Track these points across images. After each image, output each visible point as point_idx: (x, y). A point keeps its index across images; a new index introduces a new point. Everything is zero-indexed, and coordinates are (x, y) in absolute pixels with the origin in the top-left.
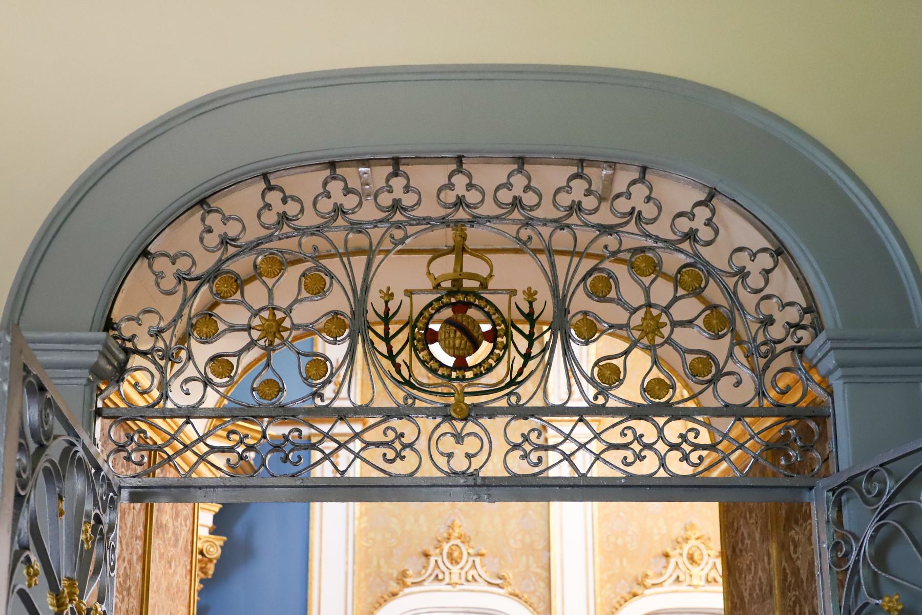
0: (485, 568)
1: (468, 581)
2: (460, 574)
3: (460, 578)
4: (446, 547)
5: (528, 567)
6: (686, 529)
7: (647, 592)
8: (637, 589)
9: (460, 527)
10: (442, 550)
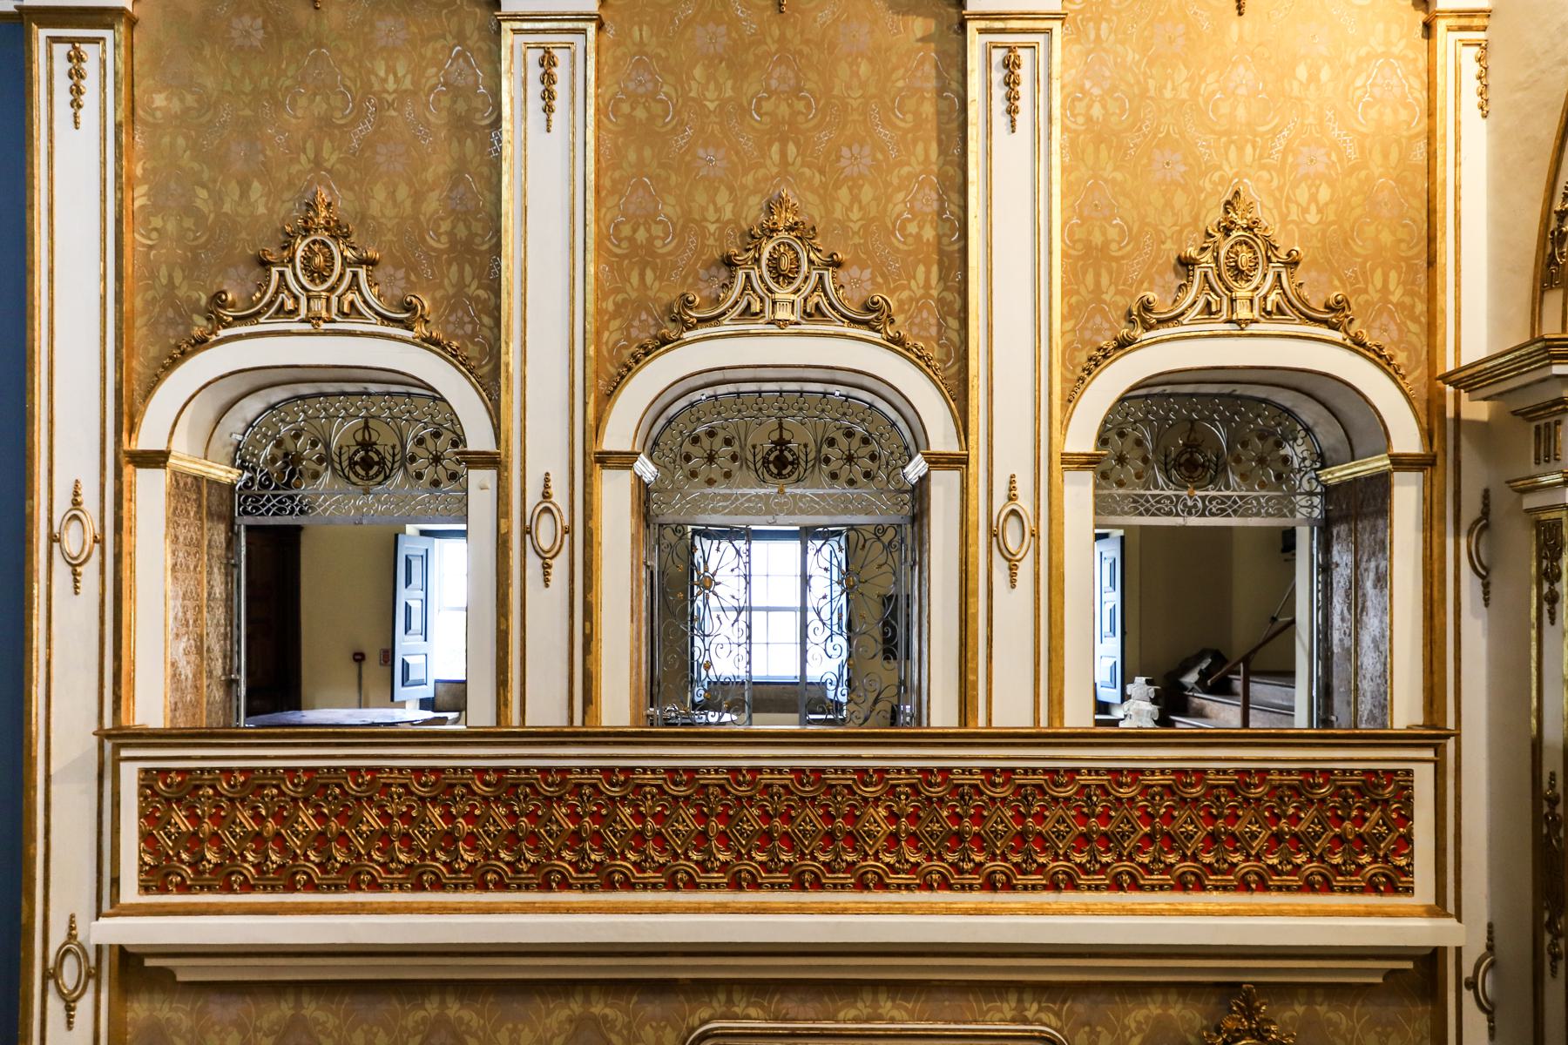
0: (376, 290)
1: (345, 315)
2: (328, 299)
3: (328, 309)
4: (301, 248)
5: (461, 285)
6: (770, 211)
7: (687, 335)
8: (670, 330)
9: (329, 204)
10: (294, 253)
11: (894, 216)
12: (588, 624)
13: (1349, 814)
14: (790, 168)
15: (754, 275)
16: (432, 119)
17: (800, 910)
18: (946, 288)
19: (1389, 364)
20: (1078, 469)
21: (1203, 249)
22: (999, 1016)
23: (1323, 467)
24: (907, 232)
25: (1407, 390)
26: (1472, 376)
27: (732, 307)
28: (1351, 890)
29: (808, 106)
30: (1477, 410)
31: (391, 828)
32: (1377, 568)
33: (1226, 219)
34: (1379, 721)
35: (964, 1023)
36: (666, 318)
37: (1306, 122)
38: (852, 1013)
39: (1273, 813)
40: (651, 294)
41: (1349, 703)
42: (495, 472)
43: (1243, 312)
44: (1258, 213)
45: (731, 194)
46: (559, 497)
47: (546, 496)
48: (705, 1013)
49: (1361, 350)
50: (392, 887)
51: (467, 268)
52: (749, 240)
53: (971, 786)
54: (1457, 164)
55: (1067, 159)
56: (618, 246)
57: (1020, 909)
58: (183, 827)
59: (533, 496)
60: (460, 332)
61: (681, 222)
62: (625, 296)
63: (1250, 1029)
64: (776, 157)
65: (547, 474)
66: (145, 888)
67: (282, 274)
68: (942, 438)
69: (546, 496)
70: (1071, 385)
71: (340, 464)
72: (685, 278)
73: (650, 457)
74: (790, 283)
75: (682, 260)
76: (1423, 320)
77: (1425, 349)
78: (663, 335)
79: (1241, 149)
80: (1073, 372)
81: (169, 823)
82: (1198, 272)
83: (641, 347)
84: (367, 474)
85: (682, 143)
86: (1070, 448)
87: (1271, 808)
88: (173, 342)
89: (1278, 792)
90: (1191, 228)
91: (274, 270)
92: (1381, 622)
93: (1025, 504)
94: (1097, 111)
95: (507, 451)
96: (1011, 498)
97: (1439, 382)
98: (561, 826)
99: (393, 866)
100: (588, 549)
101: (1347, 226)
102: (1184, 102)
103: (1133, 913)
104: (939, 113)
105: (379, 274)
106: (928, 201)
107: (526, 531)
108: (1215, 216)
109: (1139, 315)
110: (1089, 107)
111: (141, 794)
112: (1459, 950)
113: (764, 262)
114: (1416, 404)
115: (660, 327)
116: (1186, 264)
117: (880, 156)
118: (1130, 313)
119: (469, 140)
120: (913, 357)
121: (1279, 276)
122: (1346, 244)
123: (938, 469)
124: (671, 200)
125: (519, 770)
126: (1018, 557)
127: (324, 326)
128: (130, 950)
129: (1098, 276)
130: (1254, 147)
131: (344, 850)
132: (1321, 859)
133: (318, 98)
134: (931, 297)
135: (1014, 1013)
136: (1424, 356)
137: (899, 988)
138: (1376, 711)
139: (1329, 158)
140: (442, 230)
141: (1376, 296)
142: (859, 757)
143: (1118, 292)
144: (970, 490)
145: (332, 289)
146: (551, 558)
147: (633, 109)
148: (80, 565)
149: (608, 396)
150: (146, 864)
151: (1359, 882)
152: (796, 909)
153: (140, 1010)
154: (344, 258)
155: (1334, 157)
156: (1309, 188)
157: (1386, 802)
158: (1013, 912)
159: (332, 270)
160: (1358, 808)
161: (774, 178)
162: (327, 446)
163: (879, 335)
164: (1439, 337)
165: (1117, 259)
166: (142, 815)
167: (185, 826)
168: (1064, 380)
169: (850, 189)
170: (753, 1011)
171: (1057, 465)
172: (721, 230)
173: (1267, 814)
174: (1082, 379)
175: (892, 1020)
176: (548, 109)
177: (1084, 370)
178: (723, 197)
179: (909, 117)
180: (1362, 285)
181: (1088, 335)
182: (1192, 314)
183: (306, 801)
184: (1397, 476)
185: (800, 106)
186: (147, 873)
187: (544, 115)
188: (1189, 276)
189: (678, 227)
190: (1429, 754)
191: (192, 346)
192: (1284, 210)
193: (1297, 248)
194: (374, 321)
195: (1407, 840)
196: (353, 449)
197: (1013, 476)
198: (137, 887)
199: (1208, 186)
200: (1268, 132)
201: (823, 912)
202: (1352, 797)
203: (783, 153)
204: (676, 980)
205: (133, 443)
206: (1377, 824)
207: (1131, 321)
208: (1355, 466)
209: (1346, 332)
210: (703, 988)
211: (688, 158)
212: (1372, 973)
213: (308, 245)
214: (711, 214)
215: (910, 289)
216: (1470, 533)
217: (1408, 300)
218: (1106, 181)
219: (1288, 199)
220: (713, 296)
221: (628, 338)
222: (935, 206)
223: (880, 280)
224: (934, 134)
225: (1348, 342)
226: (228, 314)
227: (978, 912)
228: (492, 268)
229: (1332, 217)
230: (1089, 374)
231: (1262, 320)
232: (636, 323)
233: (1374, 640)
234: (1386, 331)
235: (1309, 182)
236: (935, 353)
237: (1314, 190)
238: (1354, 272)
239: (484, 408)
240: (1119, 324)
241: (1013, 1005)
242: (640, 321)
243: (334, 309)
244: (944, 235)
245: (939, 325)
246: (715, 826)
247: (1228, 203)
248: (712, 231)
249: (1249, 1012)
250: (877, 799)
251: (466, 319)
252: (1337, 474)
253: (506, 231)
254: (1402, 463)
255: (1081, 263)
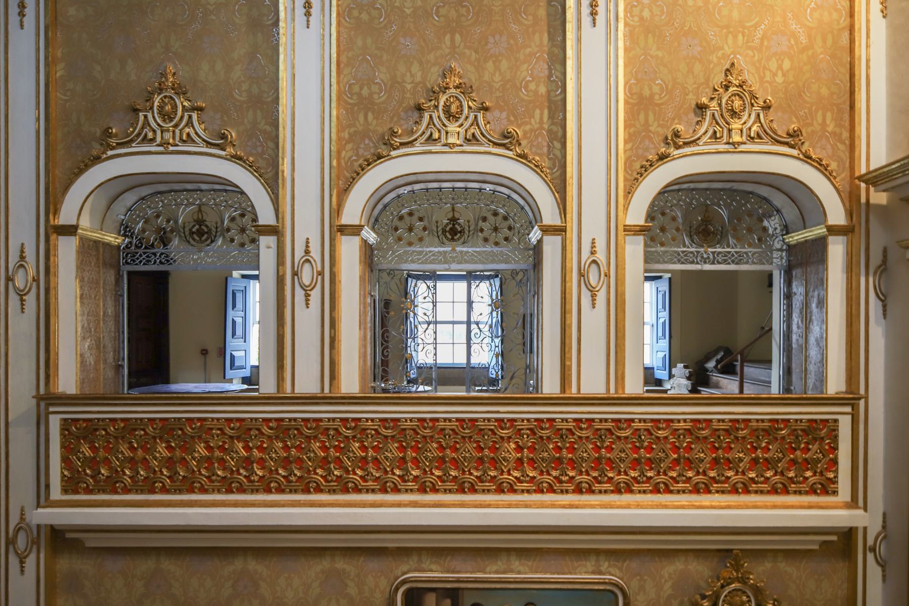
0: (203, 126)
1: (184, 141)
2: (174, 132)
3: (174, 138)
7: (394, 153)
8: (383, 150)
9: (174, 74)
10: (153, 104)
11: (521, 79)
12: (333, 331)
13: (799, 446)
14: (457, 50)
15: (435, 115)
16: (237, 20)
17: (462, 505)
18: (553, 124)
19: (826, 170)
20: (634, 235)
21: (712, 99)
22: (584, 569)
23: (787, 233)
24: (529, 89)
25: (837, 185)
26: (875, 177)
27: (421, 136)
28: (798, 492)
29: (468, 11)
30: (879, 198)
31: (212, 455)
32: (819, 295)
33: (726, 80)
34: (819, 390)
35: (563, 574)
36: (381, 143)
37: (776, 20)
38: (495, 568)
39: (752, 446)
40: (371, 128)
41: (801, 379)
42: (276, 237)
43: (736, 138)
44: (746, 76)
45: (420, 66)
46: (315, 253)
47: (307, 252)
48: (405, 568)
49: (809, 161)
50: (213, 491)
51: (258, 111)
52: (432, 94)
53: (567, 429)
54: (868, 46)
55: (628, 43)
56: (351, 98)
57: (598, 505)
58: (87, 454)
59: (299, 253)
60: (254, 152)
61: (390, 82)
62: (356, 129)
63: (738, 577)
64: (448, 43)
65: (308, 239)
66: (65, 491)
67: (146, 117)
68: (549, 215)
69: (307, 252)
70: (630, 183)
71: (184, 233)
72: (392, 118)
73: (373, 229)
74: (457, 121)
75: (390, 106)
76: (847, 142)
77: (848, 160)
78: (379, 153)
79: (735, 37)
80: (631, 175)
81: (79, 452)
82: (708, 113)
83: (366, 160)
84: (200, 239)
85: (390, 34)
86: (630, 221)
87: (751, 443)
88: (80, 159)
89: (756, 433)
90: (704, 86)
91: (141, 114)
92: (821, 328)
93: (601, 256)
94: (646, 14)
95: (283, 224)
96: (593, 253)
97: (857, 181)
98: (316, 454)
99: (214, 478)
100: (333, 284)
101: (801, 84)
102: (700, 8)
103: (666, 507)
104: (549, 15)
105: (205, 116)
106: (542, 69)
107: (295, 274)
108: (719, 78)
109: (672, 140)
110: (642, 11)
111: (62, 434)
112: (865, 529)
113: (441, 108)
114: (842, 194)
115: (376, 147)
116: (701, 108)
117: (512, 42)
118: (666, 138)
119: (259, 34)
120: (532, 166)
121: (759, 115)
122: (800, 95)
123: (547, 235)
124: (383, 69)
125: (290, 420)
126: (597, 289)
127: (171, 148)
128: (57, 528)
129: (647, 116)
130: (744, 37)
131: (184, 468)
132: (782, 474)
133: (167, 9)
134: (544, 129)
135: (594, 568)
136: (847, 165)
137: (523, 553)
138: (818, 384)
139: (790, 43)
140: (243, 89)
141: (818, 128)
142: (498, 412)
143: (659, 125)
144: (567, 248)
145: (176, 126)
146: (310, 290)
147: (360, 14)
148: (25, 295)
149: (345, 191)
150: (65, 476)
151: (804, 487)
152: (459, 505)
153: (64, 564)
154: (184, 107)
155: (793, 42)
156: (777, 61)
157: (822, 439)
158: (592, 507)
159: (176, 114)
160: (805, 443)
161: (447, 55)
162: (176, 222)
163: (511, 153)
164: (857, 153)
165: (659, 105)
166: (62, 446)
167: (88, 453)
168: (626, 180)
169: (494, 62)
170: (434, 567)
171: (621, 232)
172: (414, 88)
173: (749, 446)
174: (637, 179)
175: (519, 573)
176: (308, 14)
177: (638, 174)
178: (415, 68)
179: (530, 18)
180: (810, 121)
181: (640, 152)
182: (705, 139)
183: (161, 438)
184: (831, 239)
185: (463, 11)
186: (66, 481)
187: (305, 18)
188: (703, 116)
189: (388, 87)
190: (848, 409)
191: (92, 161)
192: (762, 74)
193: (770, 98)
194: (202, 145)
195: (834, 462)
196: (192, 224)
197: (594, 239)
198: (60, 490)
199: (715, 60)
200: (752, 26)
201: (476, 506)
202: (801, 436)
203: (452, 40)
204: (387, 548)
205: (56, 221)
206: (816, 452)
207: (668, 144)
208: (806, 232)
209: (800, 150)
210: (404, 552)
211: (394, 44)
212: (812, 543)
213: (161, 99)
214: (408, 79)
215: (531, 124)
216: (875, 274)
217: (838, 130)
218: (652, 57)
219: (765, 68)
220: (410, 129)
221: (357, 155)
222: (546, 72)
223: (512, 119)
224: (546, 28)
225: (801, 156)
226: (113, 141)
227: (571, 506)
228: (274, 112)
229: (791, 79)
230: (641, 176)
231: (748, 142)
232: (362, 146)
233: (817, 340)
234: (824, 149)
235: (778, 57)
236: (546, 163)
237: (780, 62)
238: (805, 113)
239: (268, 198)
240: (659, 145)
241: (593, 563)
242: (365, 144)
243: (177, 138)
244: (552, 90)
245: (549, 146)
246: (410, 454)
247: (727, 70)
248: (409, 89)
249: (737, 567)
250: (510, 438)
251: (258, 144)
252: (796, 237)
253: (282, 89)
254: (833, 230)
255: (636, 107)
